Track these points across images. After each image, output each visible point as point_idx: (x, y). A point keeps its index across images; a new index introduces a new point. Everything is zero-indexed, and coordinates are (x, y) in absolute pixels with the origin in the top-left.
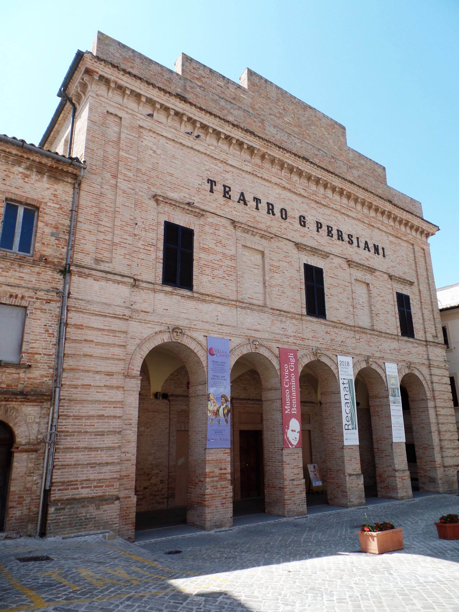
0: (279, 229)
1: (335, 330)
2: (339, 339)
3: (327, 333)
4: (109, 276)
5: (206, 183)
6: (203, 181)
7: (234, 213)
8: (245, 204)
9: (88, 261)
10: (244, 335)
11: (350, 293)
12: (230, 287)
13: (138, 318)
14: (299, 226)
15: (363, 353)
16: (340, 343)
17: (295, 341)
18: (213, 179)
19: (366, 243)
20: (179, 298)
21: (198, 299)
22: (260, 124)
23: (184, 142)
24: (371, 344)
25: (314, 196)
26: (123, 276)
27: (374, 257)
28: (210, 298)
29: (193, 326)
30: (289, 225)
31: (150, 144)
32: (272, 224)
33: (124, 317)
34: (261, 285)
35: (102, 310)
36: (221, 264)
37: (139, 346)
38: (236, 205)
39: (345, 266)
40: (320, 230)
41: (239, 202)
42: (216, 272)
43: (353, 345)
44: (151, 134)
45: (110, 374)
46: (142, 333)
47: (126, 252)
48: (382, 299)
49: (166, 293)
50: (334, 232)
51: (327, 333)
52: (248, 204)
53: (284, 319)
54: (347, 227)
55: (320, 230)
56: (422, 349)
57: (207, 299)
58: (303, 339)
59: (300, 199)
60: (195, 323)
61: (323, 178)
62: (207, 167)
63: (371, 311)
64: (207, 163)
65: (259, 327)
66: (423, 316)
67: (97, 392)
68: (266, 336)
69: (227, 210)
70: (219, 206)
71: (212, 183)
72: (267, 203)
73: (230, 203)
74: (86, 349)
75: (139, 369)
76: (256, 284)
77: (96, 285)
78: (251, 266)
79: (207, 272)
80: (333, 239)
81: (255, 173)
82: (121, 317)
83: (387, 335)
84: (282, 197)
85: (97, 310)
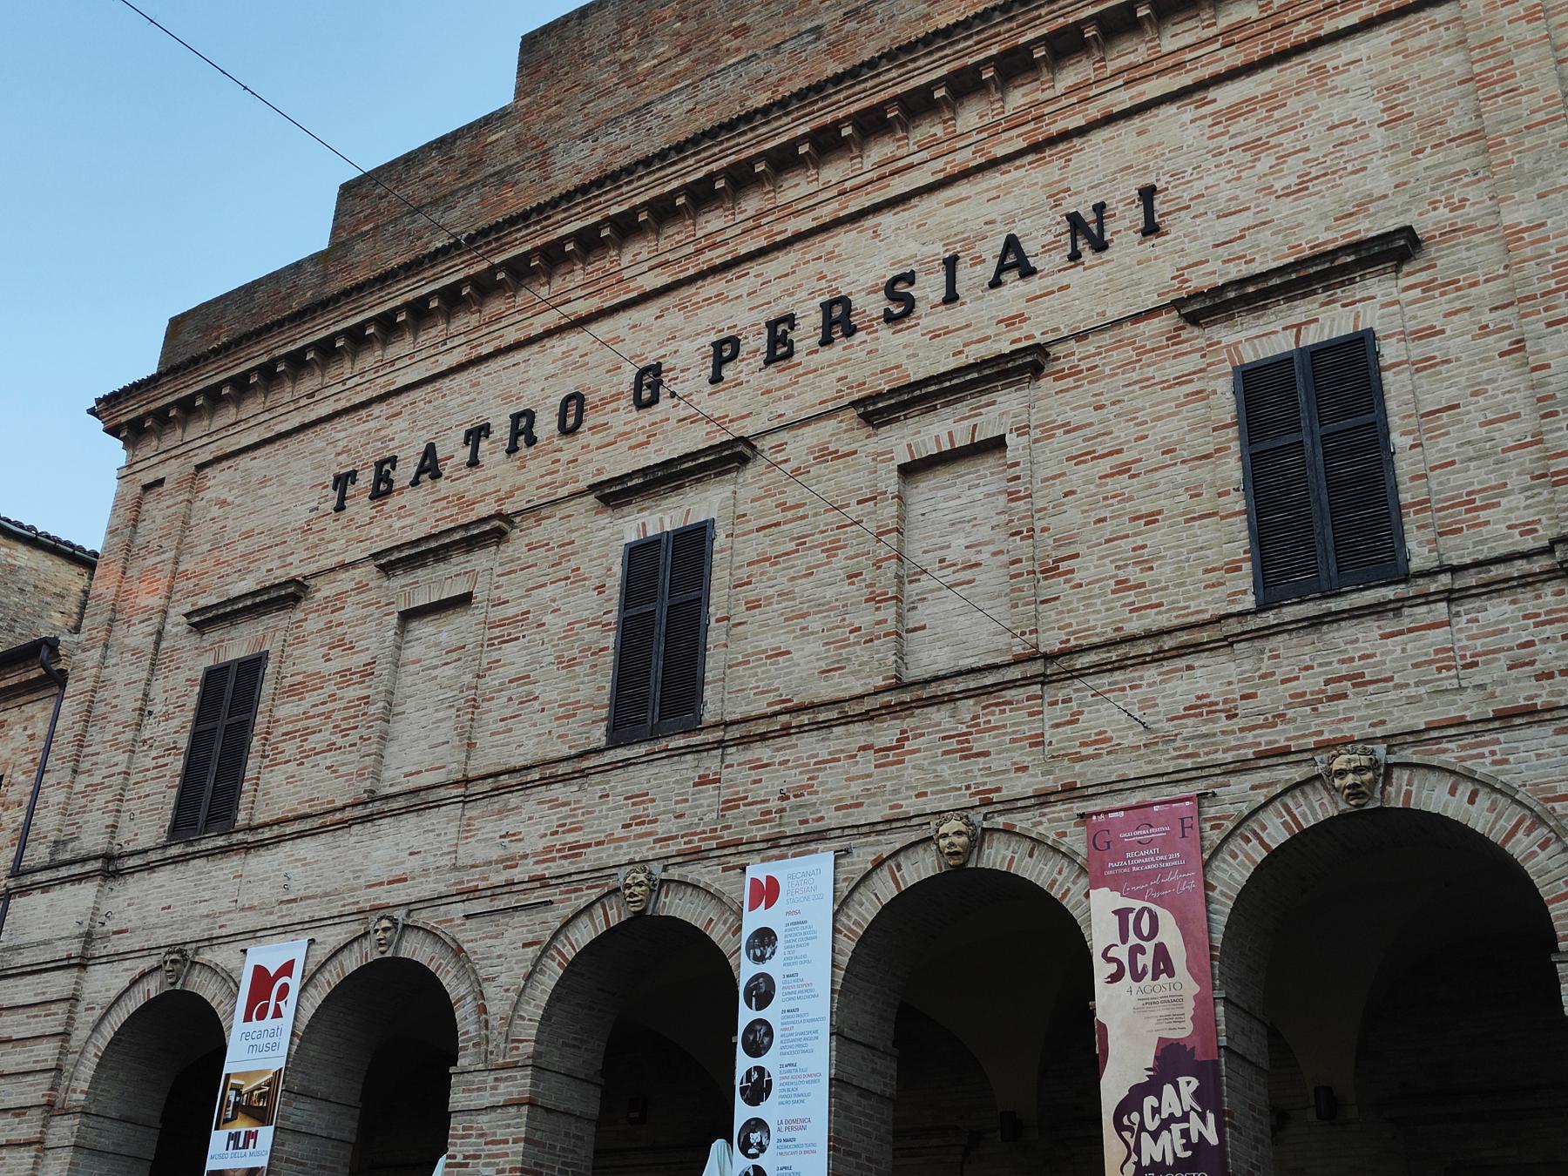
2: (771, 785)
6: (325, 492)
10: (354, 908)
12: (343, 770)
14: (635, 414)
16: (774, 804)
17: (539, 870)
21: (248, 848)
25: (708, 255)
27: (1075, 275)
28: (276, 830)
29: (216, 933)
36: (330, 706)
37: (96, 1028)
48: (1105, 466)
49: (175, 860)
51: (703, 781)
57: (267, 836)
58: (575, 850)
60: (222, 920)
61: (714, 167)
78: (435, 662)
79: (286, 756)
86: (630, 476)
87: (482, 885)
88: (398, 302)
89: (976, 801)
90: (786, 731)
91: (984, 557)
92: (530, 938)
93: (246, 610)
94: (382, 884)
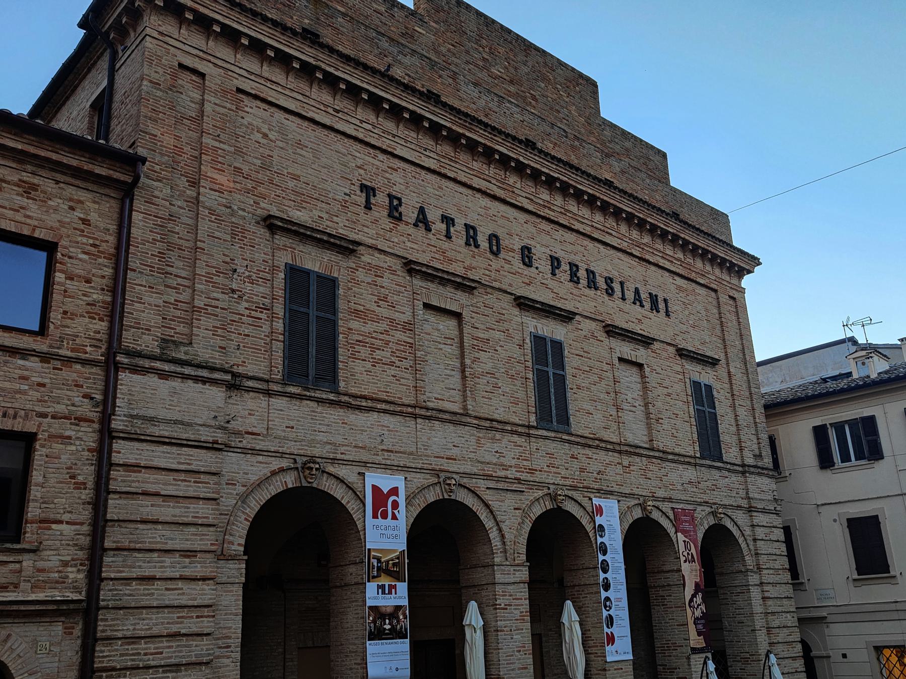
0: (487, 272)
1: (587, 451)
2: (594, 467)
3: (573, 457)
4: (187, 370)
5: (358, 192)
7: (409, 244)
8: (428, 229)
9: (149, 343)
10: (430, 467)
11: (612, 384)
13: (240, 445)
14: (522, 266)
15: (636, 491)
17: (518, 475)
18: (369, 184)
19: (637, 291)
20: (313, 404)
22: (451, 81)
23: (317, 118)
24: (650, 475)
25: (547, 211)
26: (213, 369)
27: (651, 315)
28: (370, 404)
29: (339, 456)
30: (502, 263)
31: (257, 122)
32: (474, 264)
33: (215, 446)
34: (457, 376)
35: (175, 435)
36: (387, 338)
37: (243, 499)
38: (411, 230)
39: (602, 335)
40: (557, 271)
41: (416, 225)
42: (378, 354)
43: (618, 478)
44: (259, 103)
45: (189, 553)
46: (247, 474)
47: (218, 324)
48: (665, 391)
49: (292, 396)
50: (582, 274)
51: (573, 457)
52: (433, 227)
53: (498, 436)
54: (605, 263)
55: (557, 271)
56: (735, 479)
57: (364, 404)
58: (532, 471)
59: (522, 217)
60: (343, 449)
61: (561, 177)
62: (359, 162)
63: (648, 414)
64: (358, 155)
65: (455, 452)
66: (737, 421)
67: (167, 589)
68: (468, 468)
69: (396, 240)
70: (382, 232)
71: (368, 191)
72: (465, 224)
73: (402, 227)
74: (147, 508)
75: (243, 542)
76: (448, 372)
77: (164, 387)
78: (439, 339)
79: (363, 355)
80: (580, 286)
81: (443, 171)
82: (210, 445)
83: (679, 459)
84: (491, 212)
85: (166, 434)
86: (537, 302)
87: (494, 474)
88: (411, 107)
89: (651, 495)
90: (597, 447)
91: (636, 405)
92: (516, 506)
93: (320, 241)
94: (443, 458)
